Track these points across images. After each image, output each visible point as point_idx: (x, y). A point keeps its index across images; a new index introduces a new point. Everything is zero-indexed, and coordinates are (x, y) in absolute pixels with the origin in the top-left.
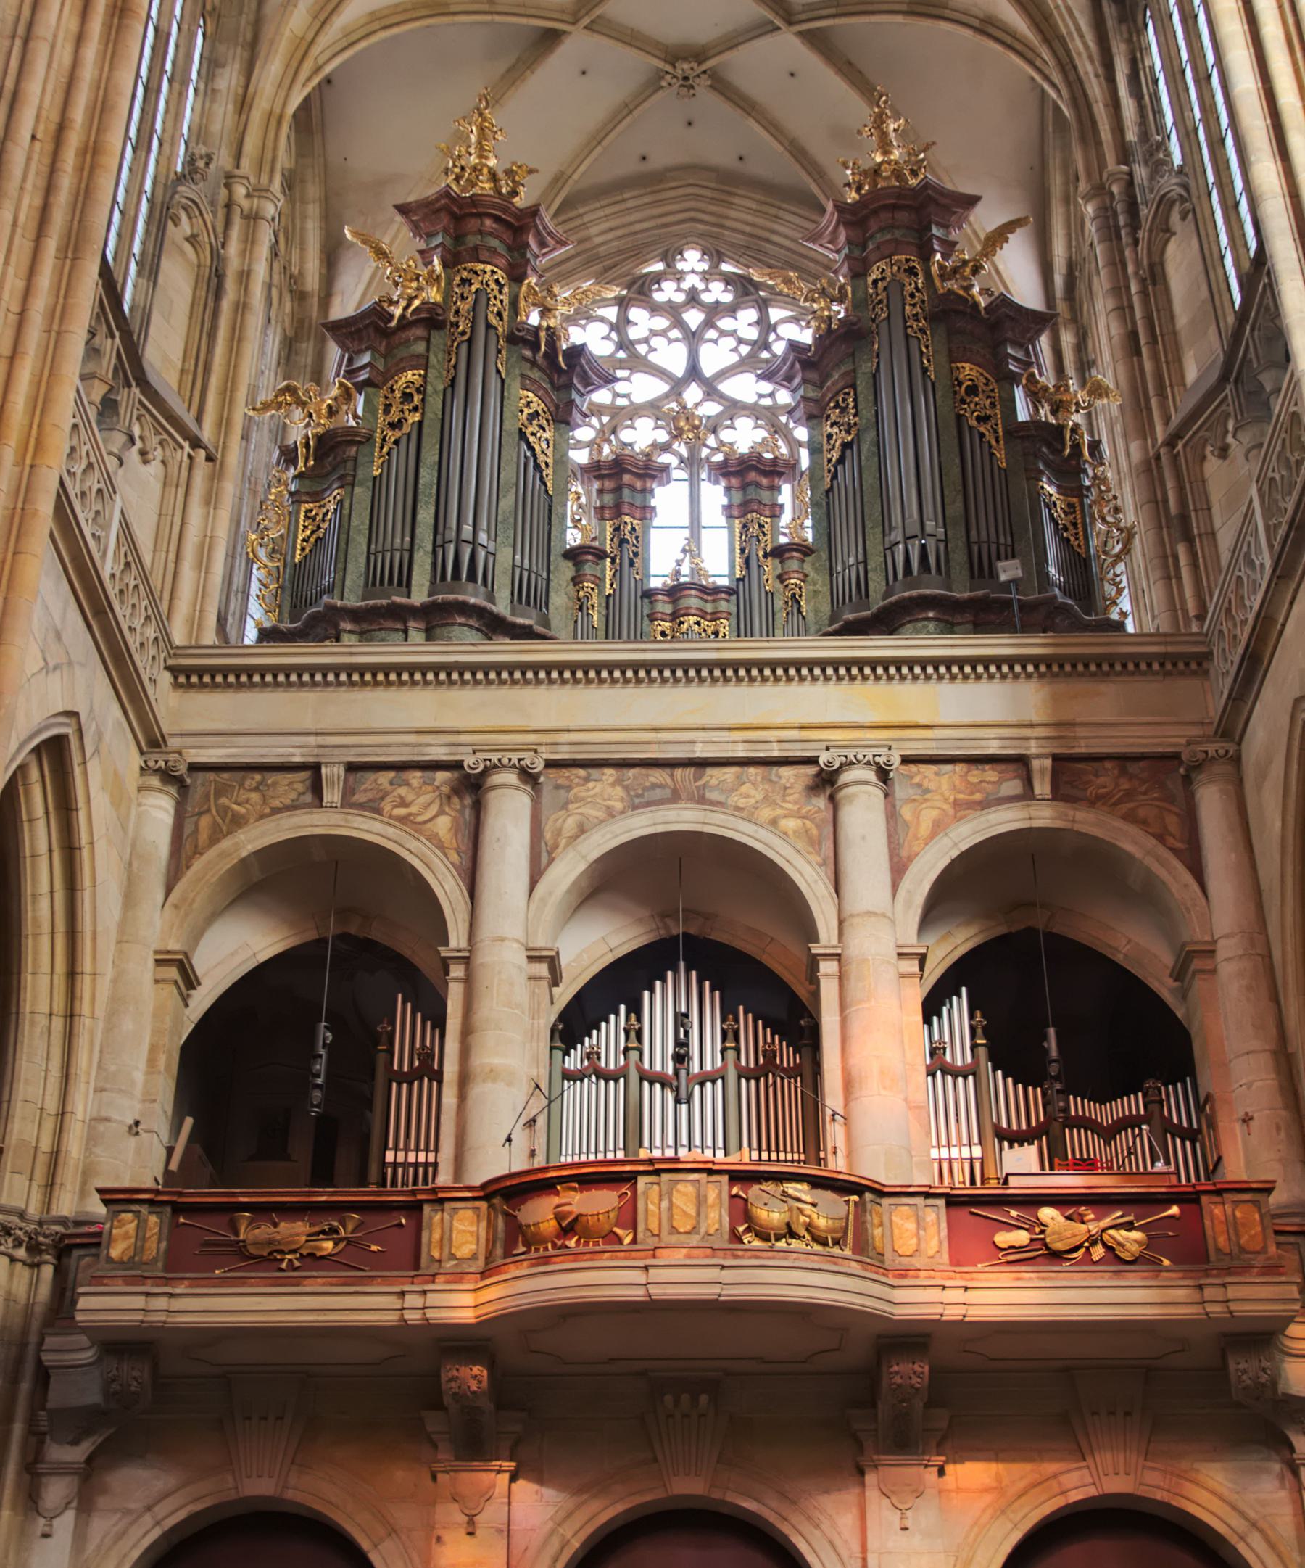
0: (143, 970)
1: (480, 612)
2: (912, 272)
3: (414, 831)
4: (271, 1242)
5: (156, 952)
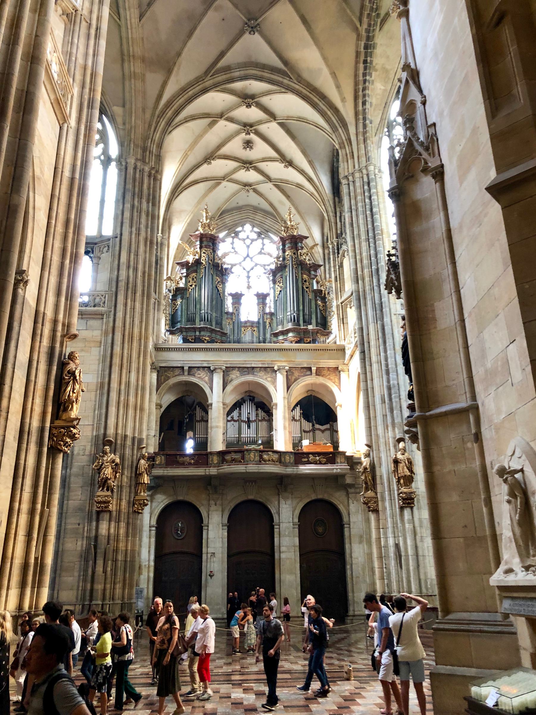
0: (154, 407)
1: (210, 328)
2: (294, 254)
3: (200, 379)
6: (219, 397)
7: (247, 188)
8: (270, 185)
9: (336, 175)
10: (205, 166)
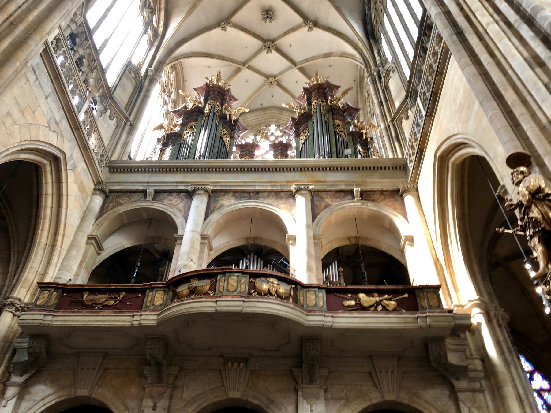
0: (83, 240)
2: (323, 102)
4: (92, 300)
5: (88, 235)
6: (196, 224)
7: (270, 79)
8: (296, 74)
9: (368, 22)
10: (218, 31)
